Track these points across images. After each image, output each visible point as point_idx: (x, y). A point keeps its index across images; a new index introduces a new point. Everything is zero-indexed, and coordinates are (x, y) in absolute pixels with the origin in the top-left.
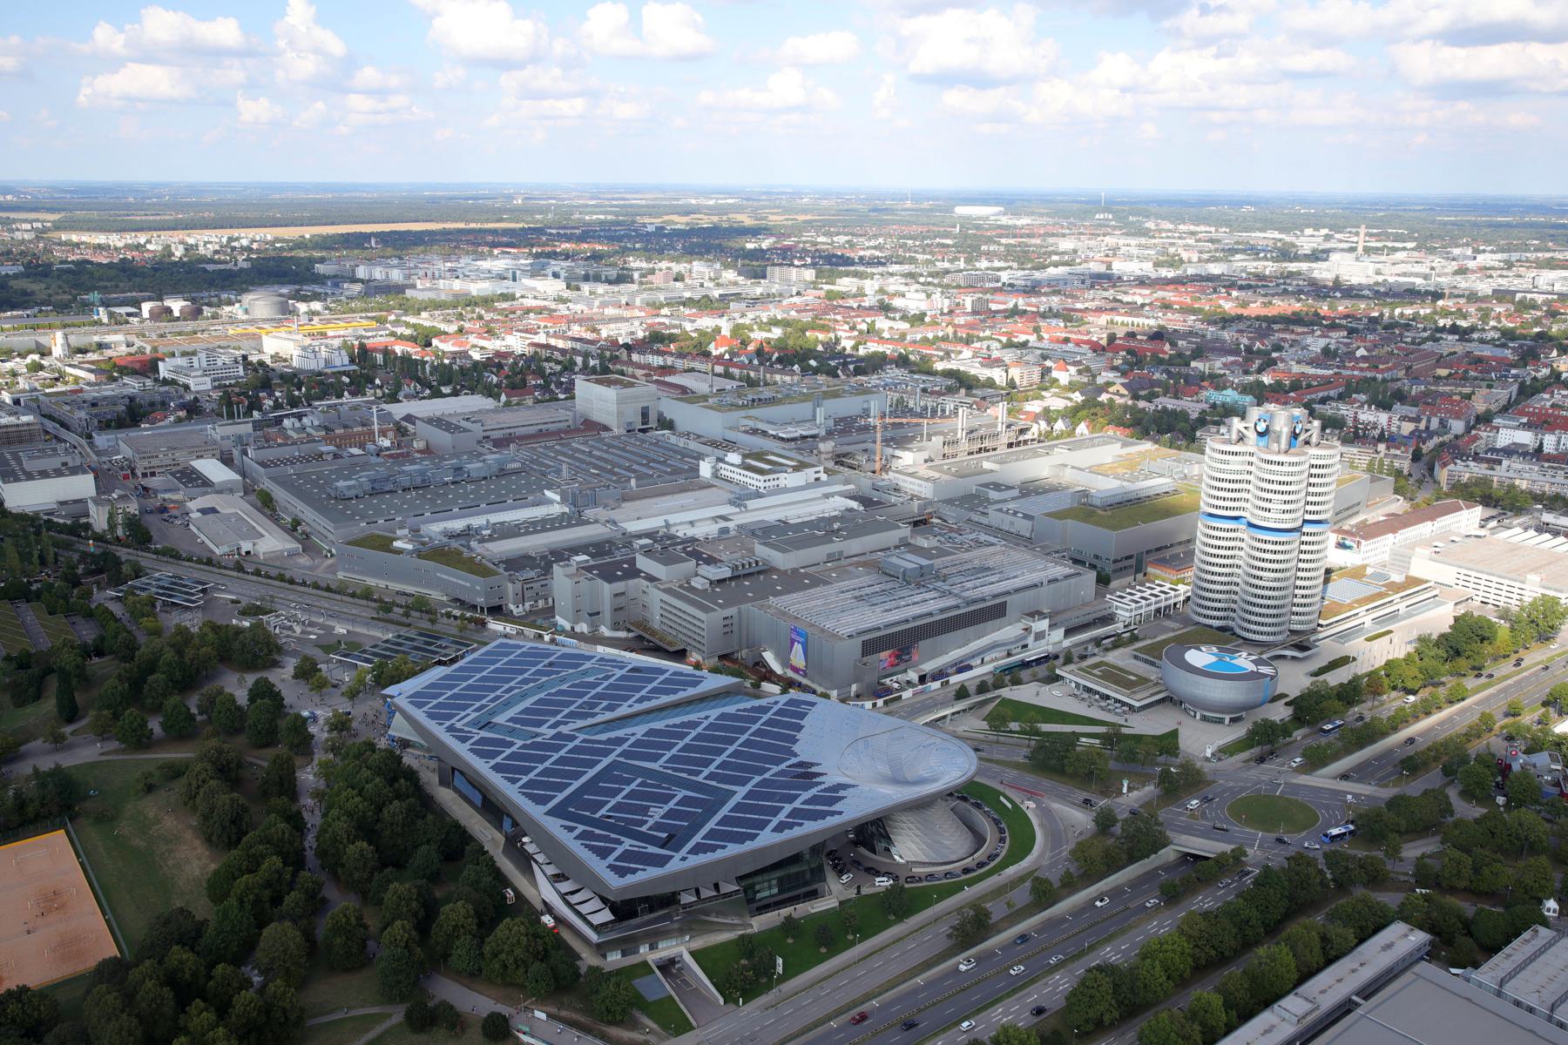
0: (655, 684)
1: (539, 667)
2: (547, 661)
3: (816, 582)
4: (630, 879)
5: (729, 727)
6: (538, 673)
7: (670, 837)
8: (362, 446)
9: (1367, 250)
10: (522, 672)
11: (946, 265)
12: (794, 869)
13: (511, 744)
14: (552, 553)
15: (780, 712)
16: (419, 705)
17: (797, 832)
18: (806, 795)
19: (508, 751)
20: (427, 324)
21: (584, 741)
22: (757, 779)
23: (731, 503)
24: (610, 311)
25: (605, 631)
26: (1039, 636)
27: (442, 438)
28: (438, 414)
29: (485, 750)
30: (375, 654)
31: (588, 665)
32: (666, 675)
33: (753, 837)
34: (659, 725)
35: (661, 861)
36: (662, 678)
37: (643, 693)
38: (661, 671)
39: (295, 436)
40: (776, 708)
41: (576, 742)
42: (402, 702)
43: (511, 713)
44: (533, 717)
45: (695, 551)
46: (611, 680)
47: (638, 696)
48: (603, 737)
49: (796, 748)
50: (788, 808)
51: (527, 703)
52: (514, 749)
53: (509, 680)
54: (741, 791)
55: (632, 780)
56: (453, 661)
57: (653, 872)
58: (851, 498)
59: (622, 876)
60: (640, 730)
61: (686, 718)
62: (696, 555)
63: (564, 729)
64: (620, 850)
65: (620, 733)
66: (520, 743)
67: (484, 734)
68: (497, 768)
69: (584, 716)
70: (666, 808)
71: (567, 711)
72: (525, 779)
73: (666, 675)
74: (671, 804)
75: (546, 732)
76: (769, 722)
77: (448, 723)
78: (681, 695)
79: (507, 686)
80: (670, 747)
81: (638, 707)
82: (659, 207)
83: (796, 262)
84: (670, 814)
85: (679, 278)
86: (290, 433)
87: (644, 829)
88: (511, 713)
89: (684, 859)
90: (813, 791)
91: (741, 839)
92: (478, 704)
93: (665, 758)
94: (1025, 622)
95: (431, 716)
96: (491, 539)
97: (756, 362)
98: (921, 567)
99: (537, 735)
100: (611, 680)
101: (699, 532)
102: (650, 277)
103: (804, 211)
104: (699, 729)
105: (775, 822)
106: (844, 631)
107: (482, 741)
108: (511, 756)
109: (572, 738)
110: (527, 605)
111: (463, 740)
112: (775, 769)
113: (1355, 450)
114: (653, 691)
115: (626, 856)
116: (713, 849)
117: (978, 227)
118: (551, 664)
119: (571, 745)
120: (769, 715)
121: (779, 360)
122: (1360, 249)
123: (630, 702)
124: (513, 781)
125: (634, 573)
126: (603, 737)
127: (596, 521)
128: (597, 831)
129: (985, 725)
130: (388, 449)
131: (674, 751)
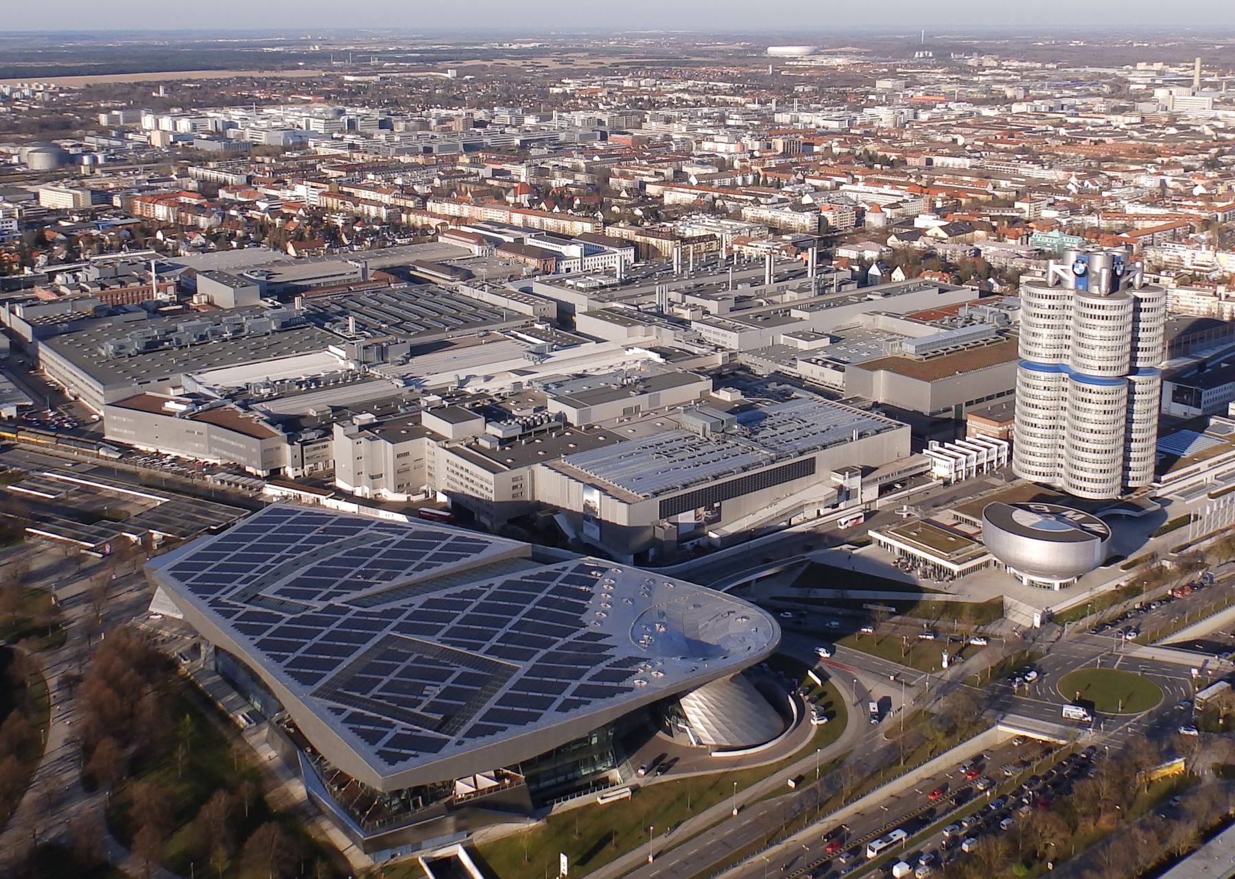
0: (436, 550)
5: (514, 595)
7: (446, 720)
9: (1204, 84)
11: (756, 106)
13: (278, 619)
16: (182, 578)
17: (583, 712)
19: (276, 626)
20: (215, 175)
21: (358, 613)
22: (543, 652)
24: (406, 159)
25: (389, 495)
27: (224, 296)
28: (223, 268)
31: (365, 531)
32: (449, 541)
33: (535, 718)
36: (444, 543)
37: (423, 560)
38: (443, 537)
39: (67, 292)
41: (349, 615)
43: (280, 584)
44: (303, 589)
46: (389, 547)
47: (418, 563)
48: (378, 609)
49: (584, 618)
50: (575, 684)
51: (298, 573)
52: (282, 623)
54: (523, 667)
58: (651, 350)
59: (392, 763)
60: (418, 601)
61: (468, 587)
63: (336, 601)
65: (396, 605)
66: (288, 617)
67: (250, 608)
68: (262, 646)
69: (359, 586)
70: (443, 686)
71: (341, 580)
72: (292, 656)
73: (449, 541)
74: (448, 682)
75: (318, 605)
76: (557, 590)
77: (212, 597)
80: (449, 618)
81: (417, 576)
82: (462, 51)
83: (601, 106)
84: (446, 694)
85: (481, 124)
86: (63, 289)
87: (417, 710)
88: (280, 584)
89: (460, 743)
90: (602, 665)
91: (522, 720)
92: (246, 575)
93: (443, 632)
94: (839, 480)
97: (556, 209)
99: (307, 608)
100: (389, 547)
101: (492, 388)
102: (449, 124)
103: (612, 53)
104: (481, 599)
108: (281, 632)
109: (344, 611)
111: (227, 615)
112: (562, 641)
113: (1192, 293)
114: (436, 557)
115: (398, 741)
116: (492, 731)
117: (791, 69)
119: (344, 618)
121: (580, 208)
122: (1196, 83)
123: (409, 570)
124: (279, 659)
125: (418, 432)
126: (378, 609)
131: (453, 623)
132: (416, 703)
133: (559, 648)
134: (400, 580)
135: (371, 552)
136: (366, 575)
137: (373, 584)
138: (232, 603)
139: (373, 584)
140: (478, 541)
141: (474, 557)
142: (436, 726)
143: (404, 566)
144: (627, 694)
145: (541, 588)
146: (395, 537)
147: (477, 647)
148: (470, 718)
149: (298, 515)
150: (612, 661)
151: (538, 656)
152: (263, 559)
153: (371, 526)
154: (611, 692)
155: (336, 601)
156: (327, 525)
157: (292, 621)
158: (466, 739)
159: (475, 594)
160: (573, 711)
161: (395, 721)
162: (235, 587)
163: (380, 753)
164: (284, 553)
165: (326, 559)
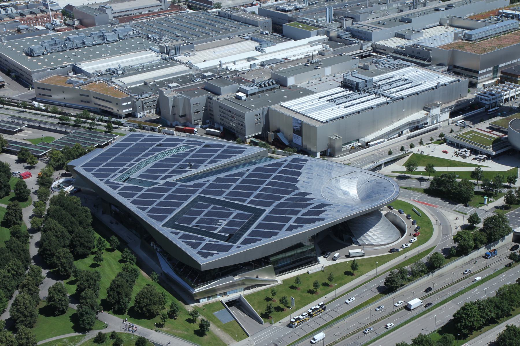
0: (218, 153)
1: (154, 146)
2: (158, 143)
3: (307, 92)
4: (210, 260)
5: (262, 174)
6: (153, 150)
8: (43, 24)
10: (145, 150)
12: (299, 251)
13: (141, 189)
14: (158, 83)
15: (288, 166)
16: (89, 170)
18: (304, 211)
19: (140, 193)
21: (181, 186)
22: (277, 203)
23: (257, 49)
26: (435, 117)
28: (86, 4)
29: (127, 193)
30: (63, 143)
31: (181, 144)
32: (224, 148)
33: (276, 234)
34: (222, 176)
35: (226, 249)
36: (222, 149)
37: (212, 158)
38: (222, 146)
40: (286, 164)
41: (177, 186)
42: (79, 168)
44: (153, 173)
45: (238, 77)
46: (194, 152)
47: (209, 160)
49: (297, 185)
50: (294, 218)
51: (149, 166)
52: (143, 192)
53: (137, 155)
54: (268, 210)
55: (209, 206)
56: (107, 144)
57: (222, 255)
59: (206, 257)
62: (239, 80)
63: (169, 180)
64: (204, 244)
66: (146, 188)
67: (126, 184)
68: (134, 203)
70: (228, 220)
71: (171, 170)
72: (150, 207)
73: (224, 148)
76: (282, 172)
78: (233, 159)
79: (137, 158)
80: (228, 187)
81: (210, 167)
84: (230, 224)
87: (216, 232)
89: (238, 247)
91: (269, 235)
92: (121, 168)
95: (96, 176)
96: (123, 76)
98: (366, 81)
99: (155, 183)
100: (194, 152)
104: (244, 177)
105: (287, 225)
106: (324, 119)
107: (125, 188)
108: (142, 196)
110: (145, 112)
111: (115, 188)
112: (287, 197)
115: (208, 247)
116: (254, 241)
118: (160, 145)
120: (282, 168)
124: (144, 209)
127: (181, 63)
128: (191, 234)
129: (405, 169)
130: (58, 26)
131: (231, 189)
132: (216, 228)
133: (286, 200)
134: (202, 169)
135: (185, 155)
136: (183, 166)
137: (188, 171)
138: (116, 182)
139: (187, 171)
140: (240, 148)
141: (239, 157)
142: (226, 239)
143: (203, 162)
144: (321, 222)
145: (274, 171)
146: (197, 147)
147: (244, 201)
148: (243, 235)
149: (145, 137)
150: (313, 206)
151: (275, 204)
152: (130, 160)
153: (184, 142)
154: (313, 221)
155: (169, 180)
156: (161, 142)
157: (148, 190)
158: (241, 245)
159: (241, 175)
160: (294, 231)
161: (205, 237)
162: (116, 174)
163: (199, 253)
164: (140, 156)
165: (162, 159)
